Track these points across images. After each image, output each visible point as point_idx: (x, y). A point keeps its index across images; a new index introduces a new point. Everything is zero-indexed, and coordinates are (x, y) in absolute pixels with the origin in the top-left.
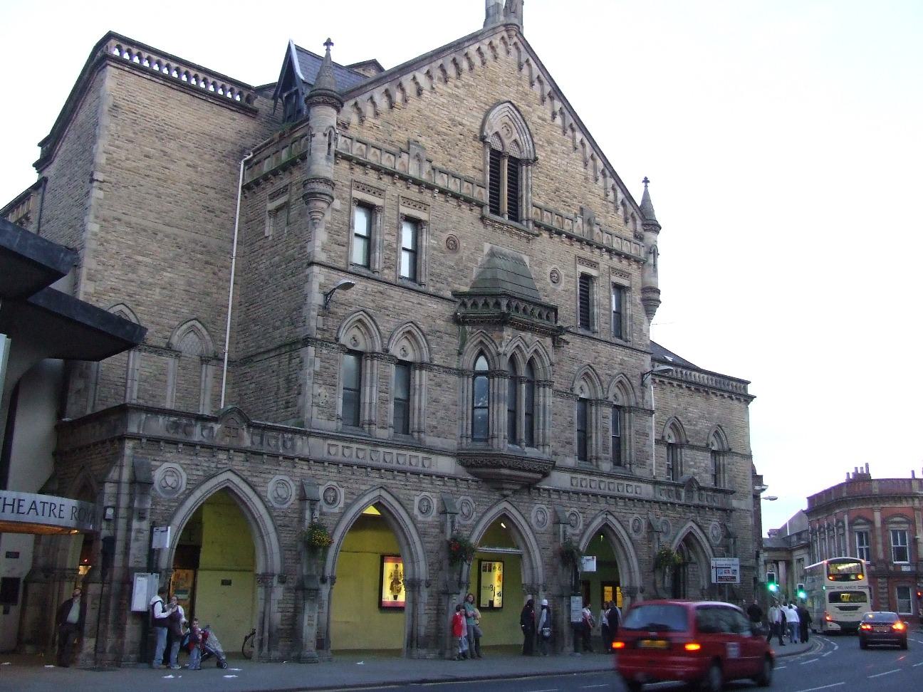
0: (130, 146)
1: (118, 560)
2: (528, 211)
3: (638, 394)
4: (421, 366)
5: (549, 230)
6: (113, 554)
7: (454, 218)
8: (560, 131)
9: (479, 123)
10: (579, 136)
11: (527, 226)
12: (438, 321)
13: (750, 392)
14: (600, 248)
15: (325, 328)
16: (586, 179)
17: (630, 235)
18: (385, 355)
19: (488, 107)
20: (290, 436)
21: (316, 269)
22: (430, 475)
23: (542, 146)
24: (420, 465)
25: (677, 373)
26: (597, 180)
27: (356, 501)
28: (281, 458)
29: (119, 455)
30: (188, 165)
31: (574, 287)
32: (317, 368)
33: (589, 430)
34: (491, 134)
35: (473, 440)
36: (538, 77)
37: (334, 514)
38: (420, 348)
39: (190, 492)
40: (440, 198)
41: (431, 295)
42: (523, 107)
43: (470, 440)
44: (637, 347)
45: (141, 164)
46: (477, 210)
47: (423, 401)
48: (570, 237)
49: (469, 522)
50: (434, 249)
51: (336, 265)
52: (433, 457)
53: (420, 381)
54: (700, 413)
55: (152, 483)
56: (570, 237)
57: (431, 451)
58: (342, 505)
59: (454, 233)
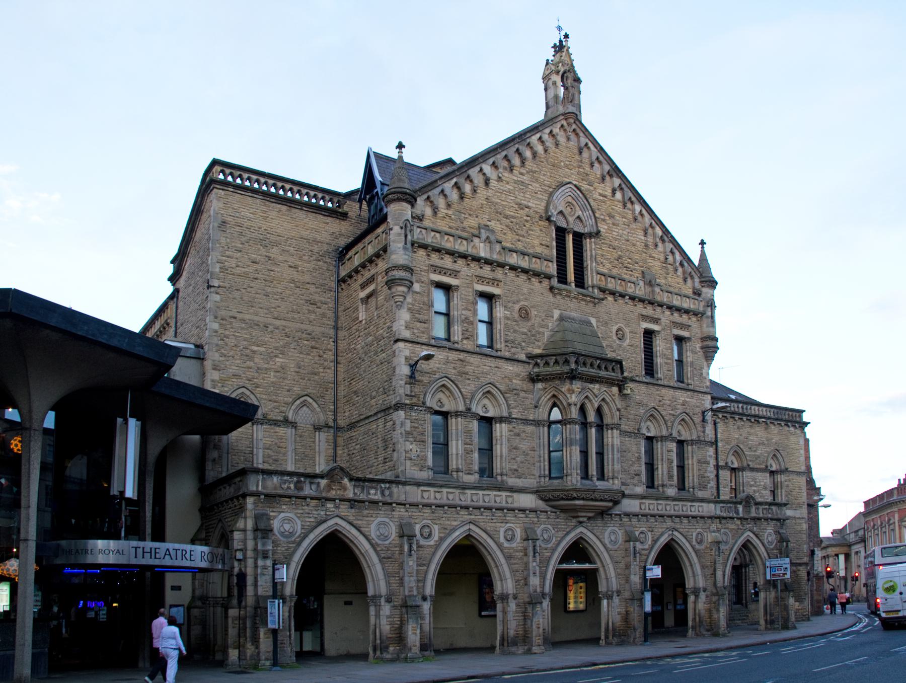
0: (239, 255)
1: (250, 590)
3: (700, 429)
4: (501, 420)
5: (613, 293)
6: (245, 586)
7: (525, 291)
8: (620, 205)
9: (544, 204)
10: (638, 208)
11: (593, 292)
12: (514, 381)
13: (805, 419)
14: (661, 305)
15: (413, 394)
16: (646, 246)
17: (689, 292)
18: (468, 413)
19: (551, 190)
20: (387, 485)
21: (401, 345)
22: (513, 510)
23: (604, 220)
24: (504, 502)
25: (735, 407)
26: (656, 246)
27: (449, 534)
28: (381, 504)
29: (242, 508)
30: (291, 267)
31: (640, 341)
32: (408, 428)
33: (655, 462)
34: (555, 213)
35: (550, 478)
36: (598, 158)
37: (431, 546)
38: (500, 405)
39: (305, 536)
40: (511, 274)
41: (507, 359)
42: (584, 186)
43: (547, 479)
44: (698, 389)
45: (250, 269)
46: (546, 282)
47: (504, 450)
48: (632, 298)
49: (549, 546)
50: (508, 319)
51: (420, 340)
52: (515, 495)
53: (501, 432)
54: (757, 439)
55: (272, 530)
56: (632, 298)
57: (512, 490)
58: (436, 538)
59: (526, 304)
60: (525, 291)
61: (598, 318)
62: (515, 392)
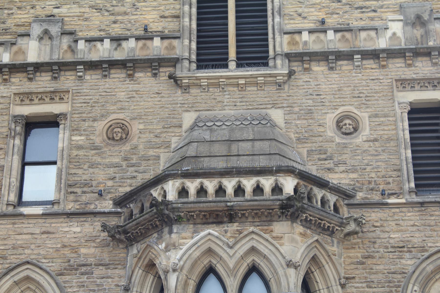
2: (279, 44)
7: (122, 95)
11: (275, 67)
50: (80, 148)
59: (121, 116)
60: (122, 95)
61: (289, 109)
62: (83, 269)
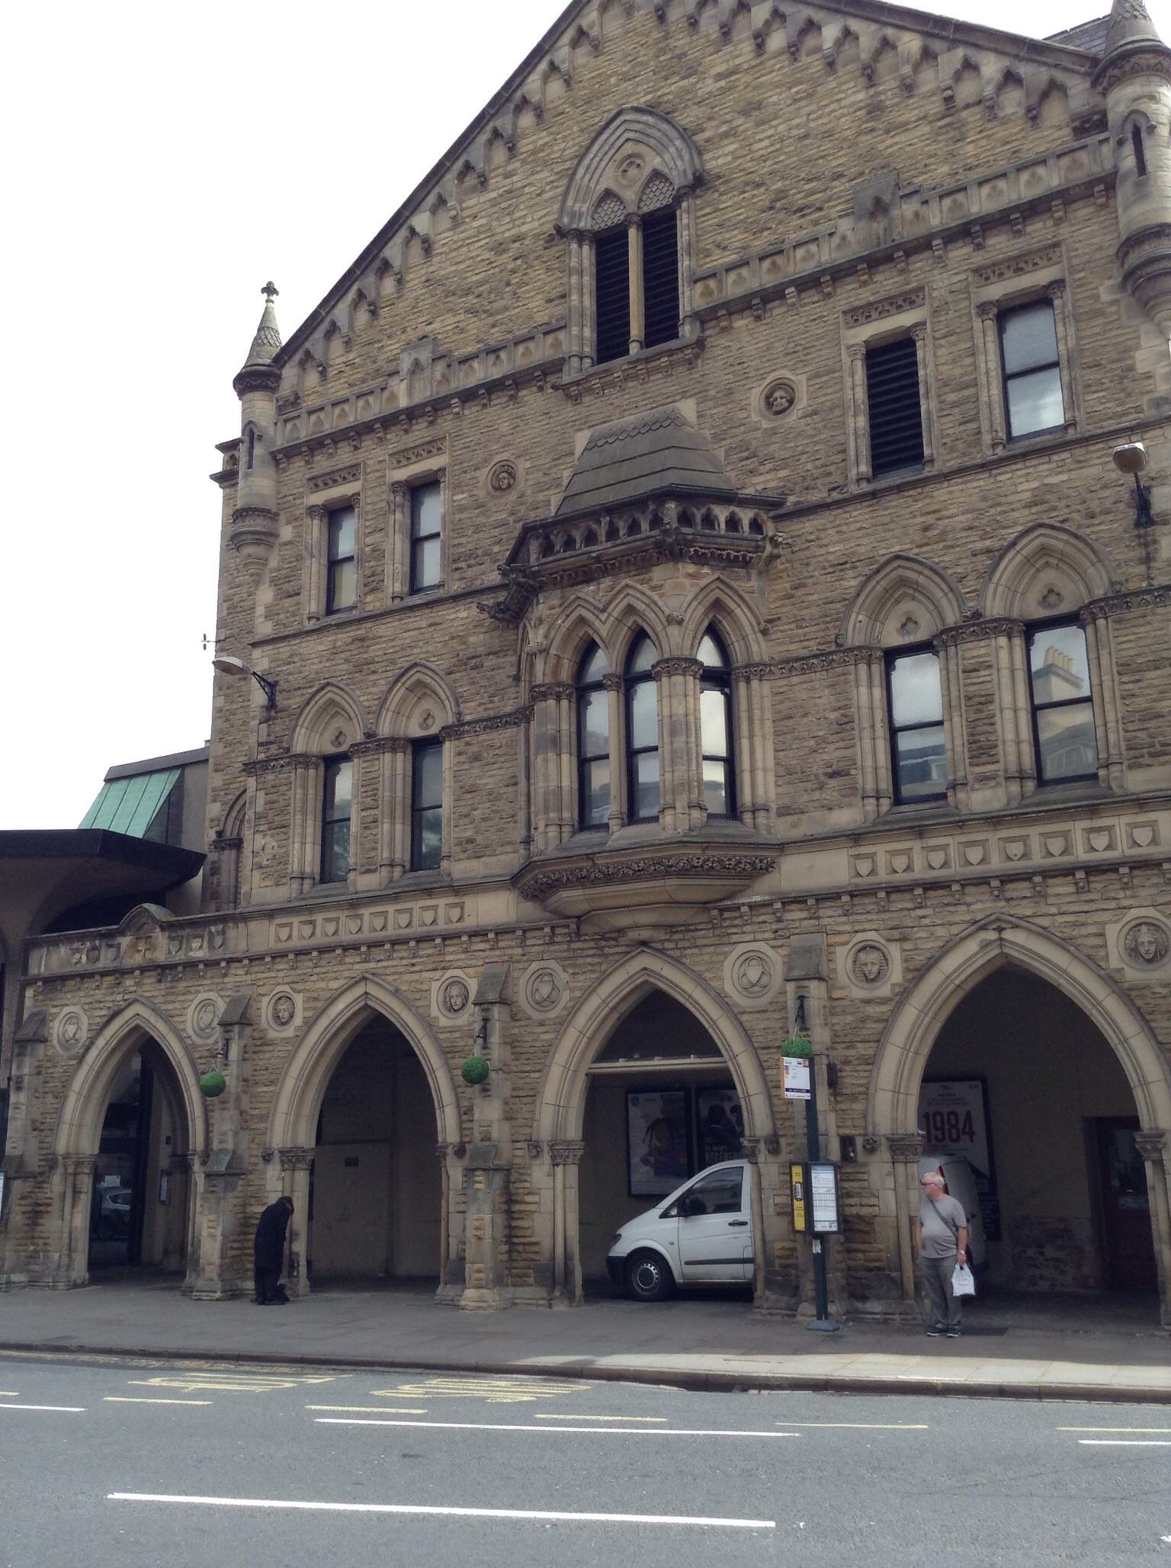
27: (323, 1012)
59: (505, 456)
60: (504, 428)
